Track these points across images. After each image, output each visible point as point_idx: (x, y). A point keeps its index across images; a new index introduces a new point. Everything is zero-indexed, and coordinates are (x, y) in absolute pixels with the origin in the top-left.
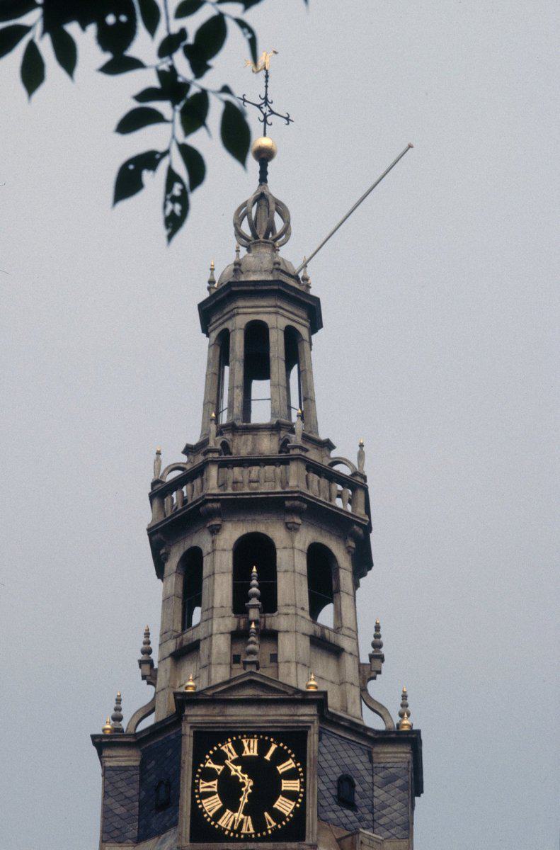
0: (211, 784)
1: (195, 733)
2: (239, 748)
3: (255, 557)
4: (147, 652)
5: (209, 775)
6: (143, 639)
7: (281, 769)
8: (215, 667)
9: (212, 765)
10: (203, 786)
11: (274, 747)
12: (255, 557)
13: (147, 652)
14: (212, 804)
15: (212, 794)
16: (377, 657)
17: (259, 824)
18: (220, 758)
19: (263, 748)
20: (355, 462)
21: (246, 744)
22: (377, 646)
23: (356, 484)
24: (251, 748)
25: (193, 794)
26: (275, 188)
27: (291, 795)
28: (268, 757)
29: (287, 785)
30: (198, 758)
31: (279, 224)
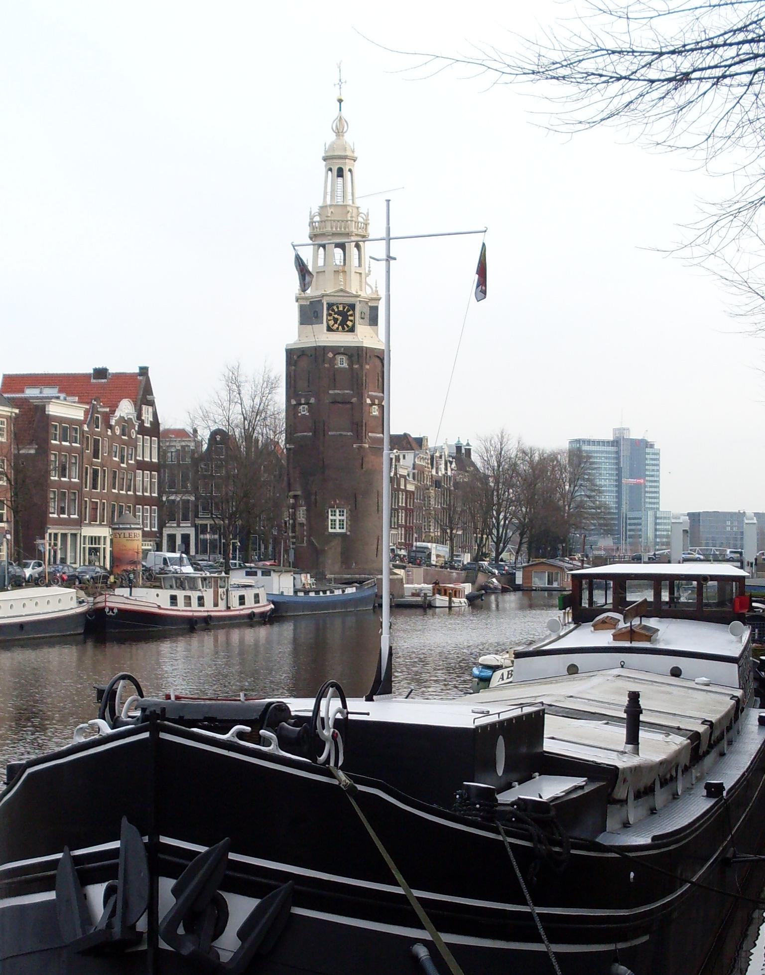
2: (338, 308)
5: (330, 315)
16: (370, 271)
17: (343, 328)
18: (333, 310)
19: (344, 308)
24: (341, 309)
26: (344, 114)
30: (328, 309)
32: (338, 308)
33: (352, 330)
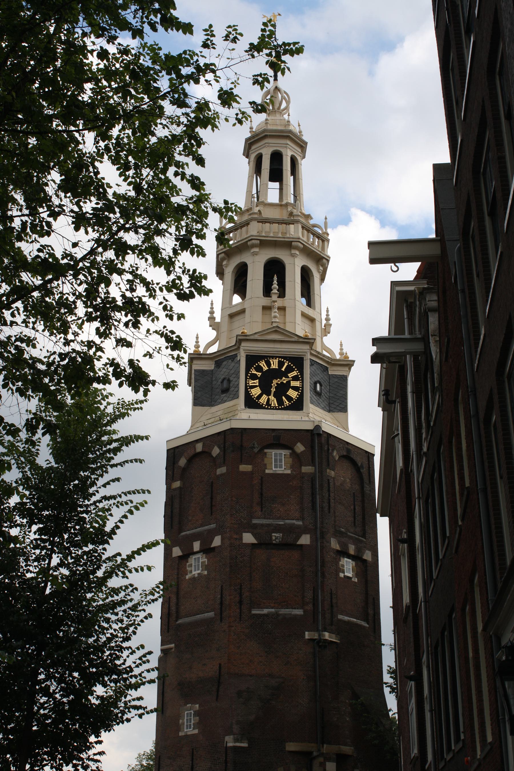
0: (255, 381)
1: (247, 356)
2: (268, 364)
3: (275, 270)
4: (212, 312)
5: (254, 377)
6: (210, 306)
7: (291, 375)
8: (253, 324)
9: (255, 372)
10: (251, 383)
11: (286, 364)
12: (275, 270)
13: (212, 312)
14: (256, 392)
15: (256, 386)
16: (328, 326)
17: (280, 402)
19: (281, 364)
20: (323, 227)
21: (272, 363)
22: (328, 319)
23: (323, 239)
24: (275, 365)
25: (246, 386)
27: (295, 389)
28: (283, 369)
29: (293, 384)
31: (284, 105)
32: (268, 364)
33: (297, 405)
